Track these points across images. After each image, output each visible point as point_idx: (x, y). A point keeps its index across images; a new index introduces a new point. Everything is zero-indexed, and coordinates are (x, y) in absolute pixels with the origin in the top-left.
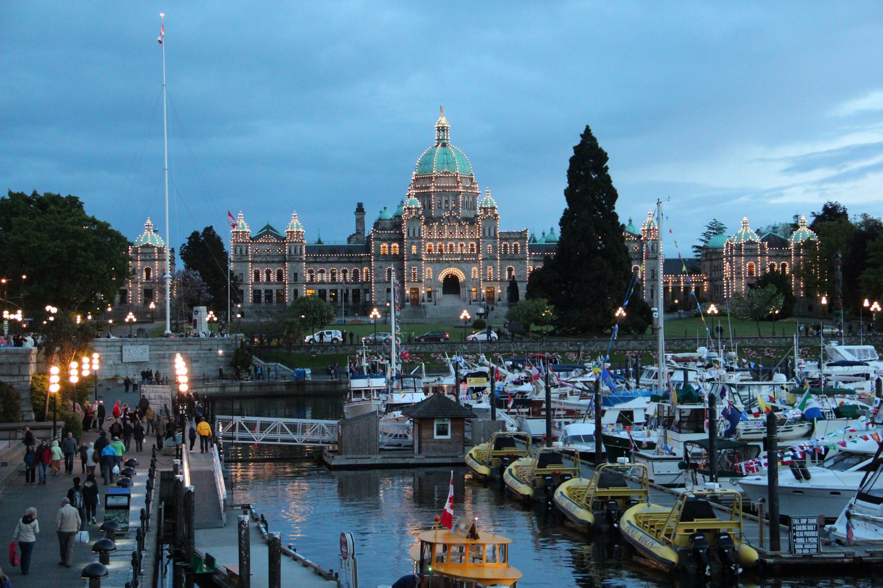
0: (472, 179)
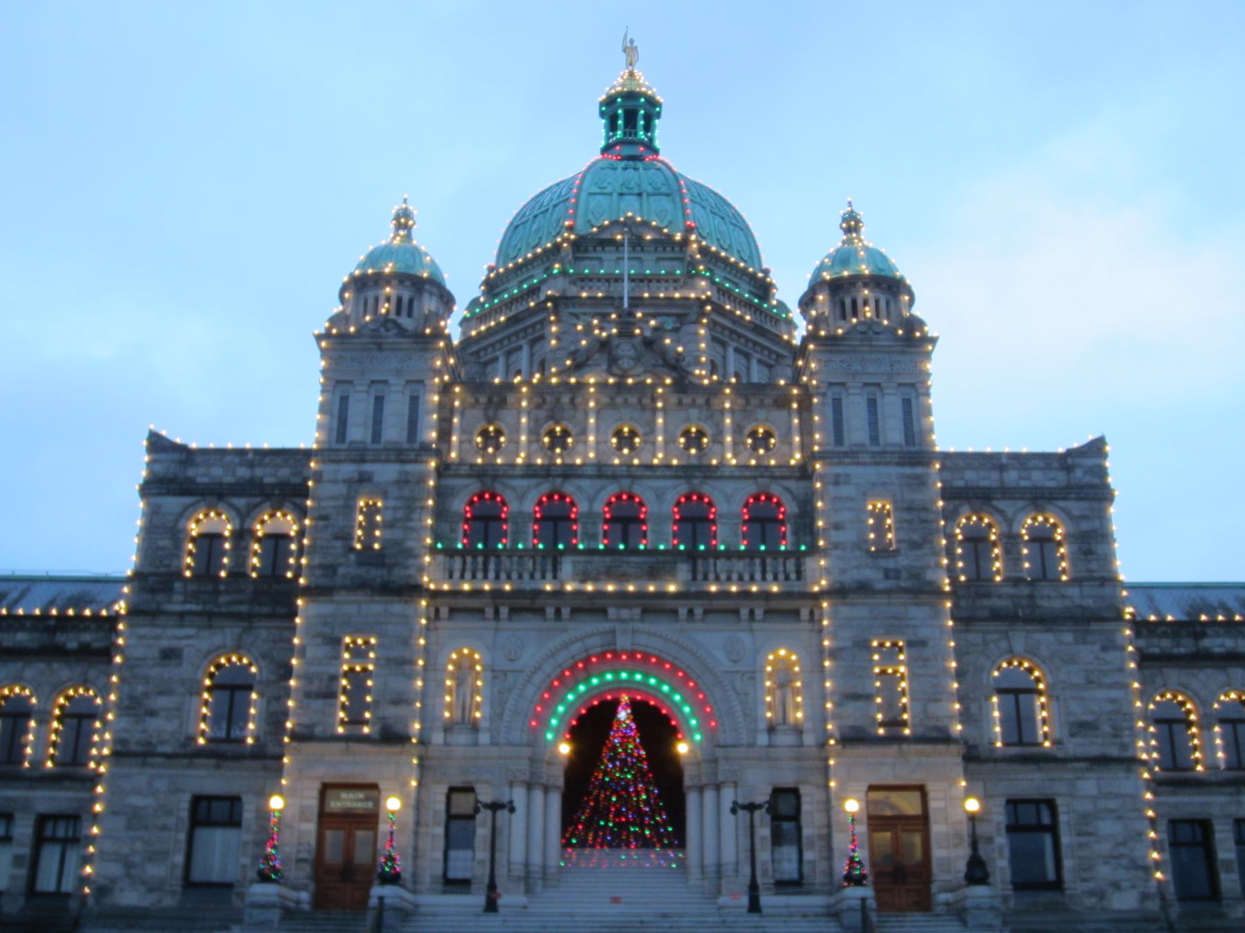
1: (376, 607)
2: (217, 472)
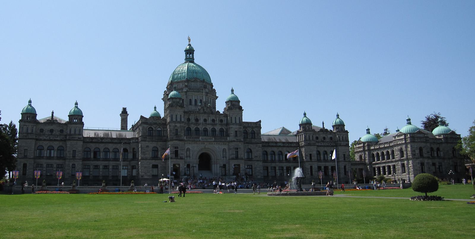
2: (151, 121)
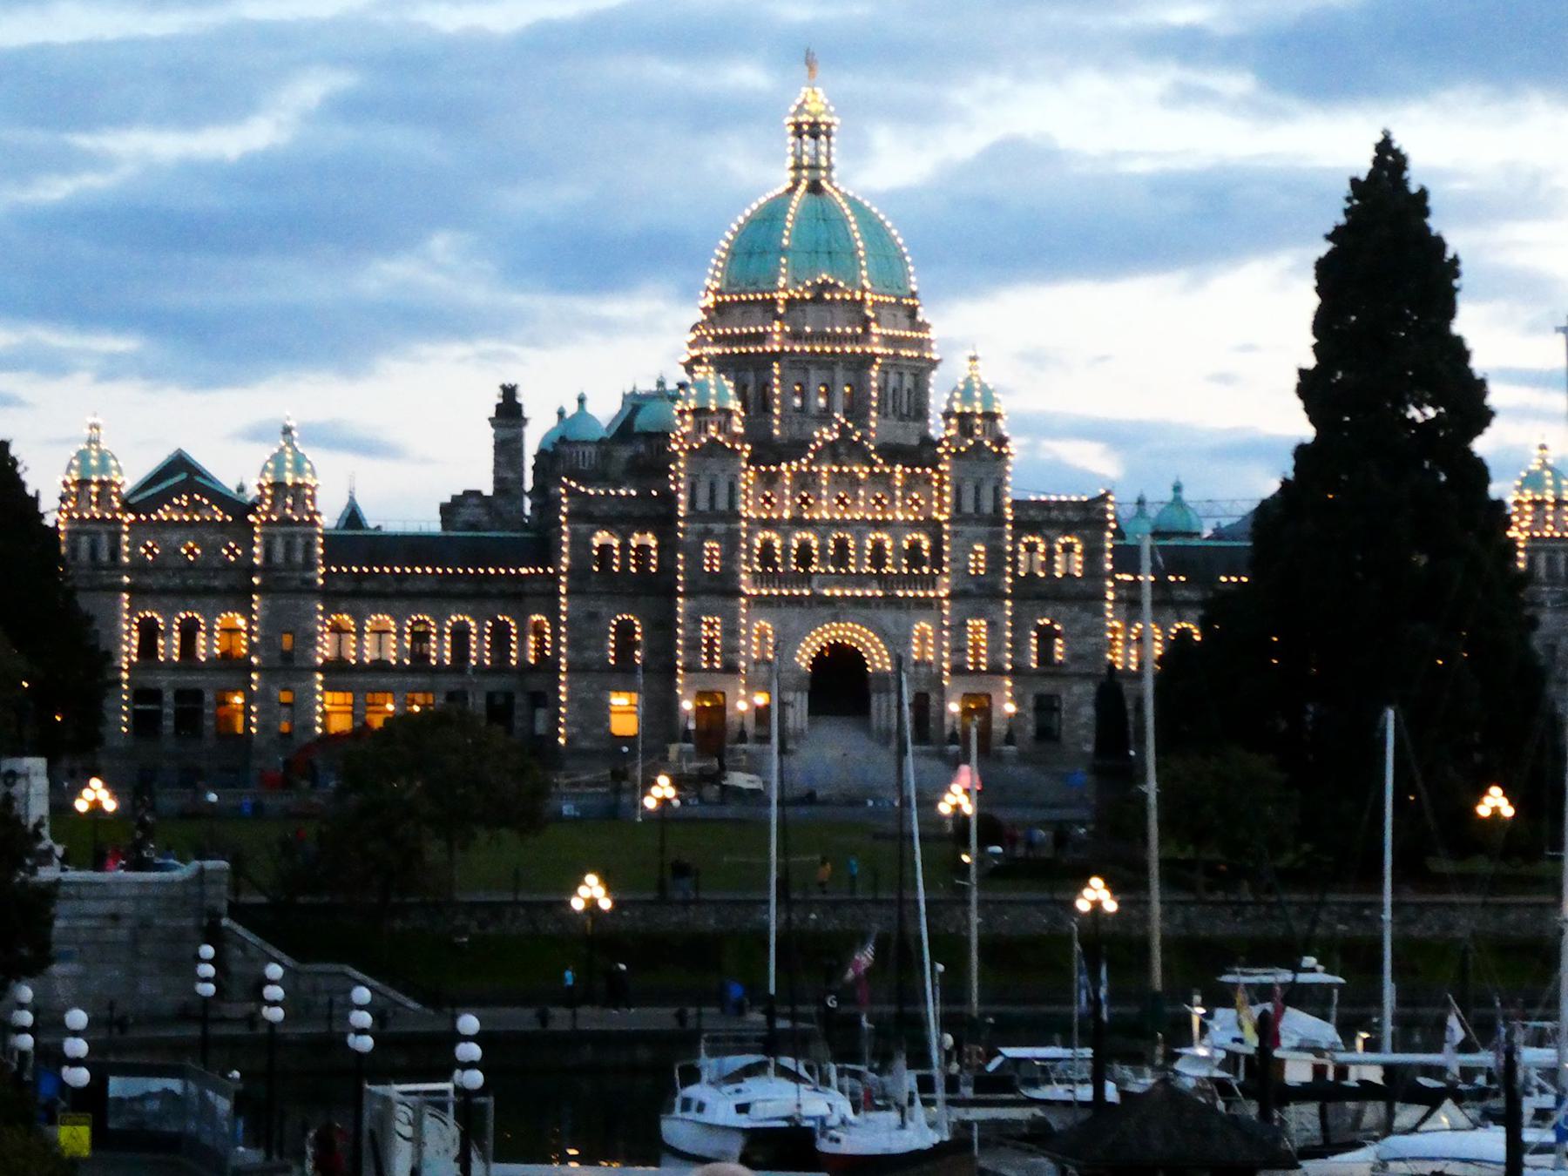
0: (912, 312)
1: (717, 602)
